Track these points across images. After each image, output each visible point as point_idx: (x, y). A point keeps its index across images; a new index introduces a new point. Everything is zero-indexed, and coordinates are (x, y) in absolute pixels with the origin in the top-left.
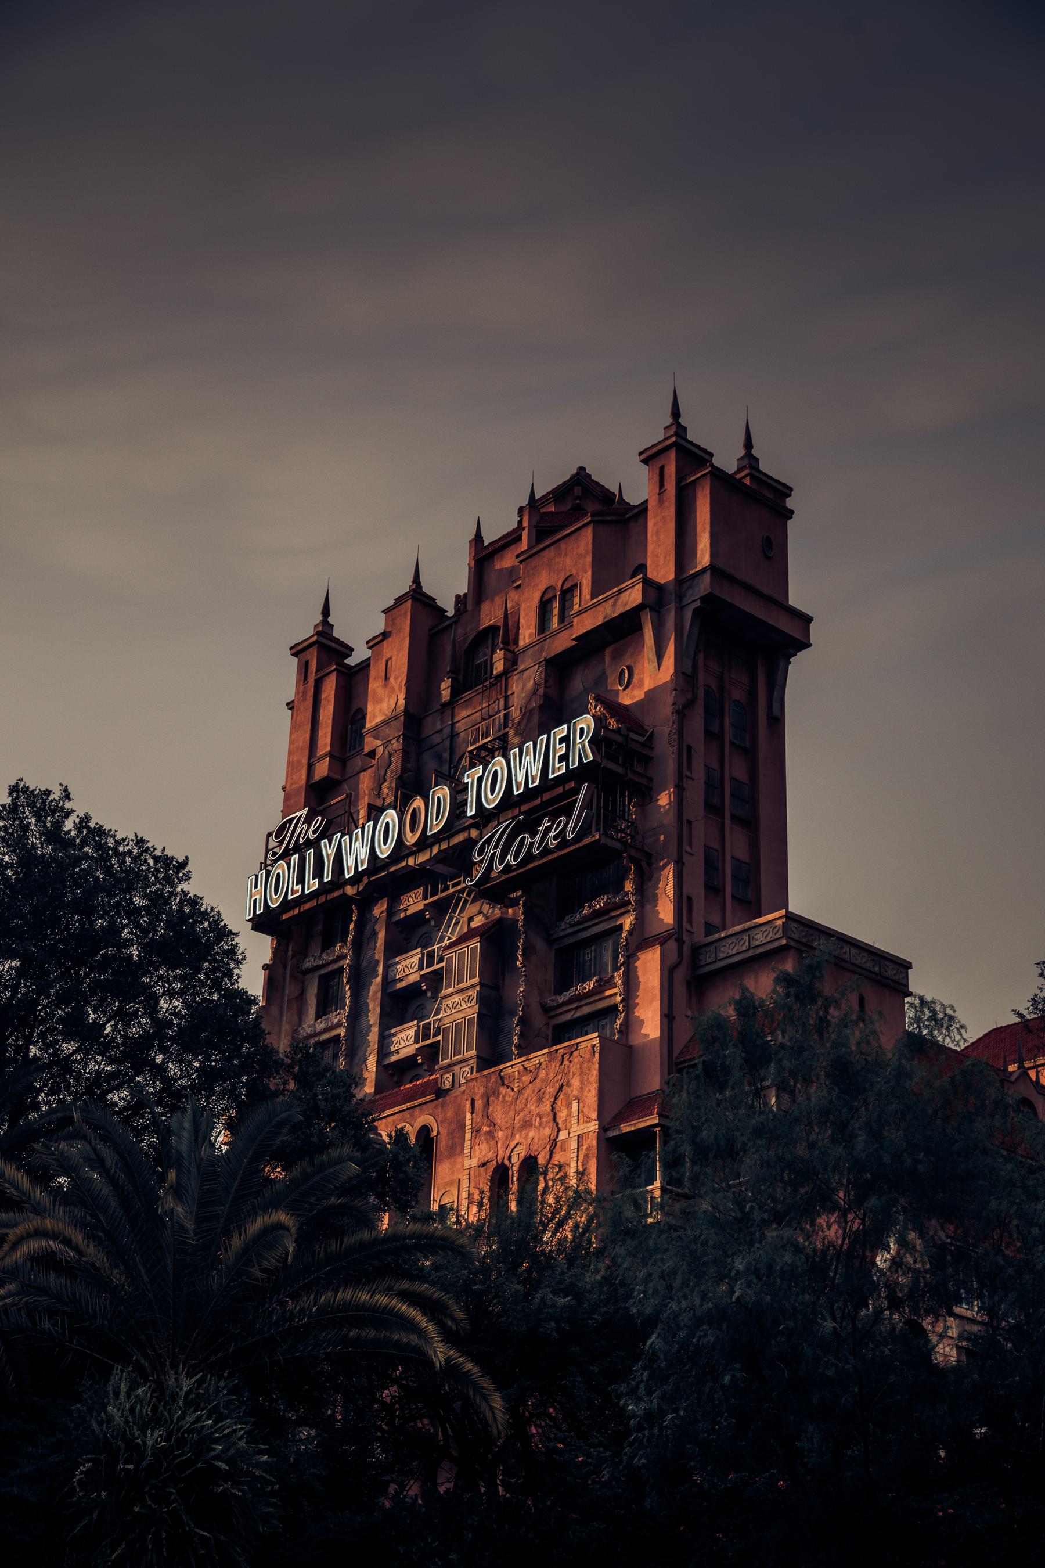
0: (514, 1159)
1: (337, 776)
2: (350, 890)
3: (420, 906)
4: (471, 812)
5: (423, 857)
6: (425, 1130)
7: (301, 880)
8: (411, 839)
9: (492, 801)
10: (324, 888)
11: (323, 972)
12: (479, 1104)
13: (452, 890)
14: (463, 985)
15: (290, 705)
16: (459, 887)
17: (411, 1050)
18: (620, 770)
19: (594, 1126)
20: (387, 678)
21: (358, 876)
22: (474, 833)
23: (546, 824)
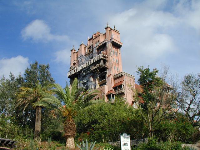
2: (78, 73)
5: (85, 69)
21: (79, 72)
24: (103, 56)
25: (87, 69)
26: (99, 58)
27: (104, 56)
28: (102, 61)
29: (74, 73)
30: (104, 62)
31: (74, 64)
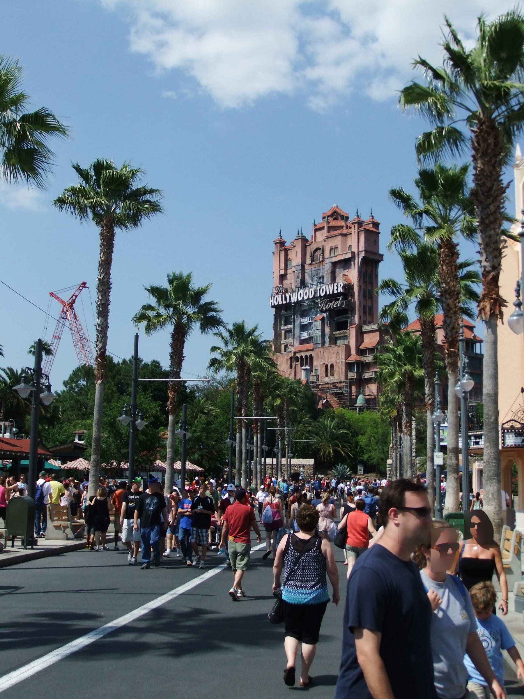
6: (311, 355)
7: (282, 300)
8: (306, 298)
9: (322, 294)
12: (322, 352)
17: (307, 337)
19: (344, 360)
21: (294, 302)
26: (337, 289)
29: (284, 302)
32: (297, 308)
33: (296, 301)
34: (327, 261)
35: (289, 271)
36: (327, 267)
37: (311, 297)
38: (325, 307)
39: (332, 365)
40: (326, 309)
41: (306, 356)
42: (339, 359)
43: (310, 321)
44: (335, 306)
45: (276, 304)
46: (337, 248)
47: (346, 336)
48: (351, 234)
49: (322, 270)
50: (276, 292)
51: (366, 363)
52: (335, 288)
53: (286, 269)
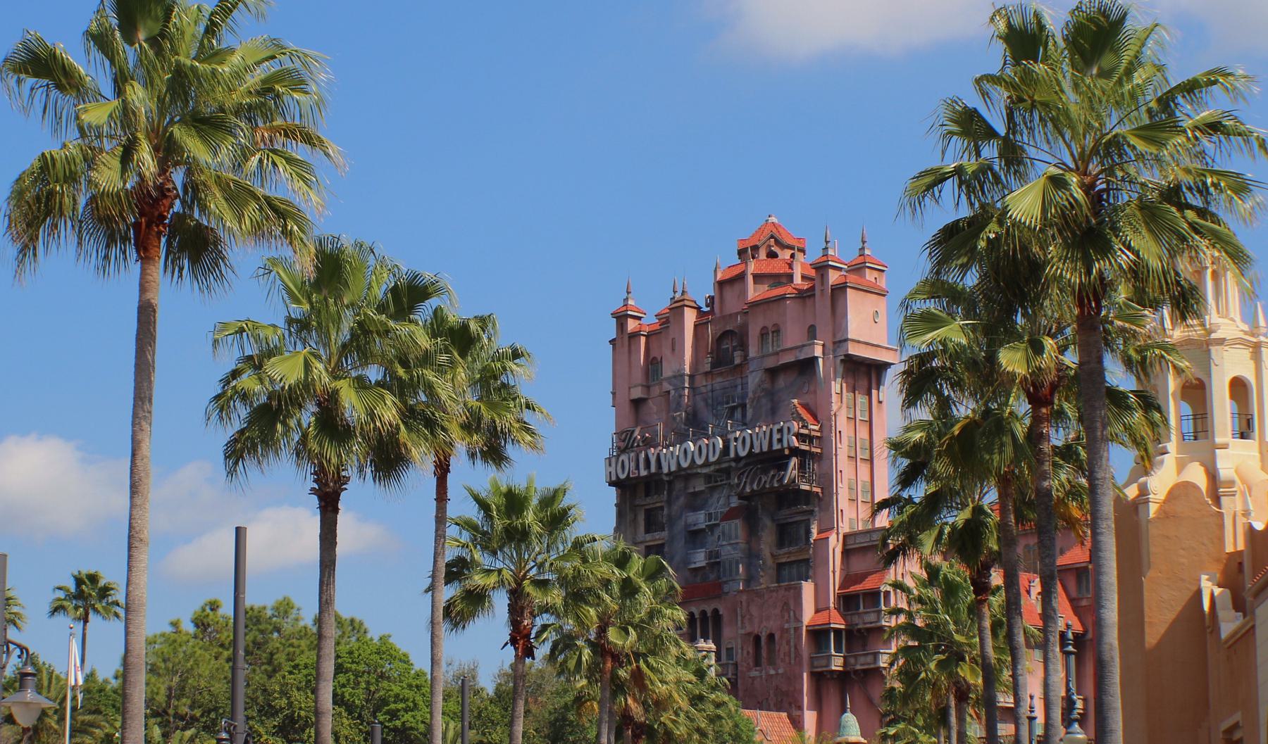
0: (764, 634)
1: (645, 396)
2: (666, 478)
3: (702, 488)
4: (732, 455)
5: (705, 471)
8: (699, 462)
9: (743, 453)
10: (650, 475)
11: (647, 507)
12: (744, 604)
13: (719, 483)
14: (732, 542)
15: (612, 342)
16: (724, 482)
17: (703, 564)
18: (807, 448)
20: (673, 350)
21: (670, 473)
22: (733, 464)
23: (772, 473)
24: (798, 435)
25: (717, 471)
26: (780, 441)
27: (802, 435)
28: (794, 461)
29: (643, 473)
30: (802, 467)
31: (637, 404)
32: (679, 485)
33: (673, 468)
34: (752, 366)
35: (656, 391)
36: (754, 379)
37: (712, 459)
38: (752, 484)
39: (771, 637)
40: (753, 490)
41: (703, 613)
42: (788, 622)
43: (713, 522)
44: (776, 485)
45: (623, 476)
46: (779, 331)
47: (807, 560)
48: (814, 295)
49: (740, 387)
50: (623, 445)
51: (859, 630)
52: (776, 436)
53: (647, 387)
